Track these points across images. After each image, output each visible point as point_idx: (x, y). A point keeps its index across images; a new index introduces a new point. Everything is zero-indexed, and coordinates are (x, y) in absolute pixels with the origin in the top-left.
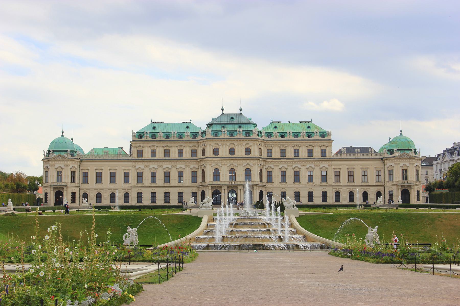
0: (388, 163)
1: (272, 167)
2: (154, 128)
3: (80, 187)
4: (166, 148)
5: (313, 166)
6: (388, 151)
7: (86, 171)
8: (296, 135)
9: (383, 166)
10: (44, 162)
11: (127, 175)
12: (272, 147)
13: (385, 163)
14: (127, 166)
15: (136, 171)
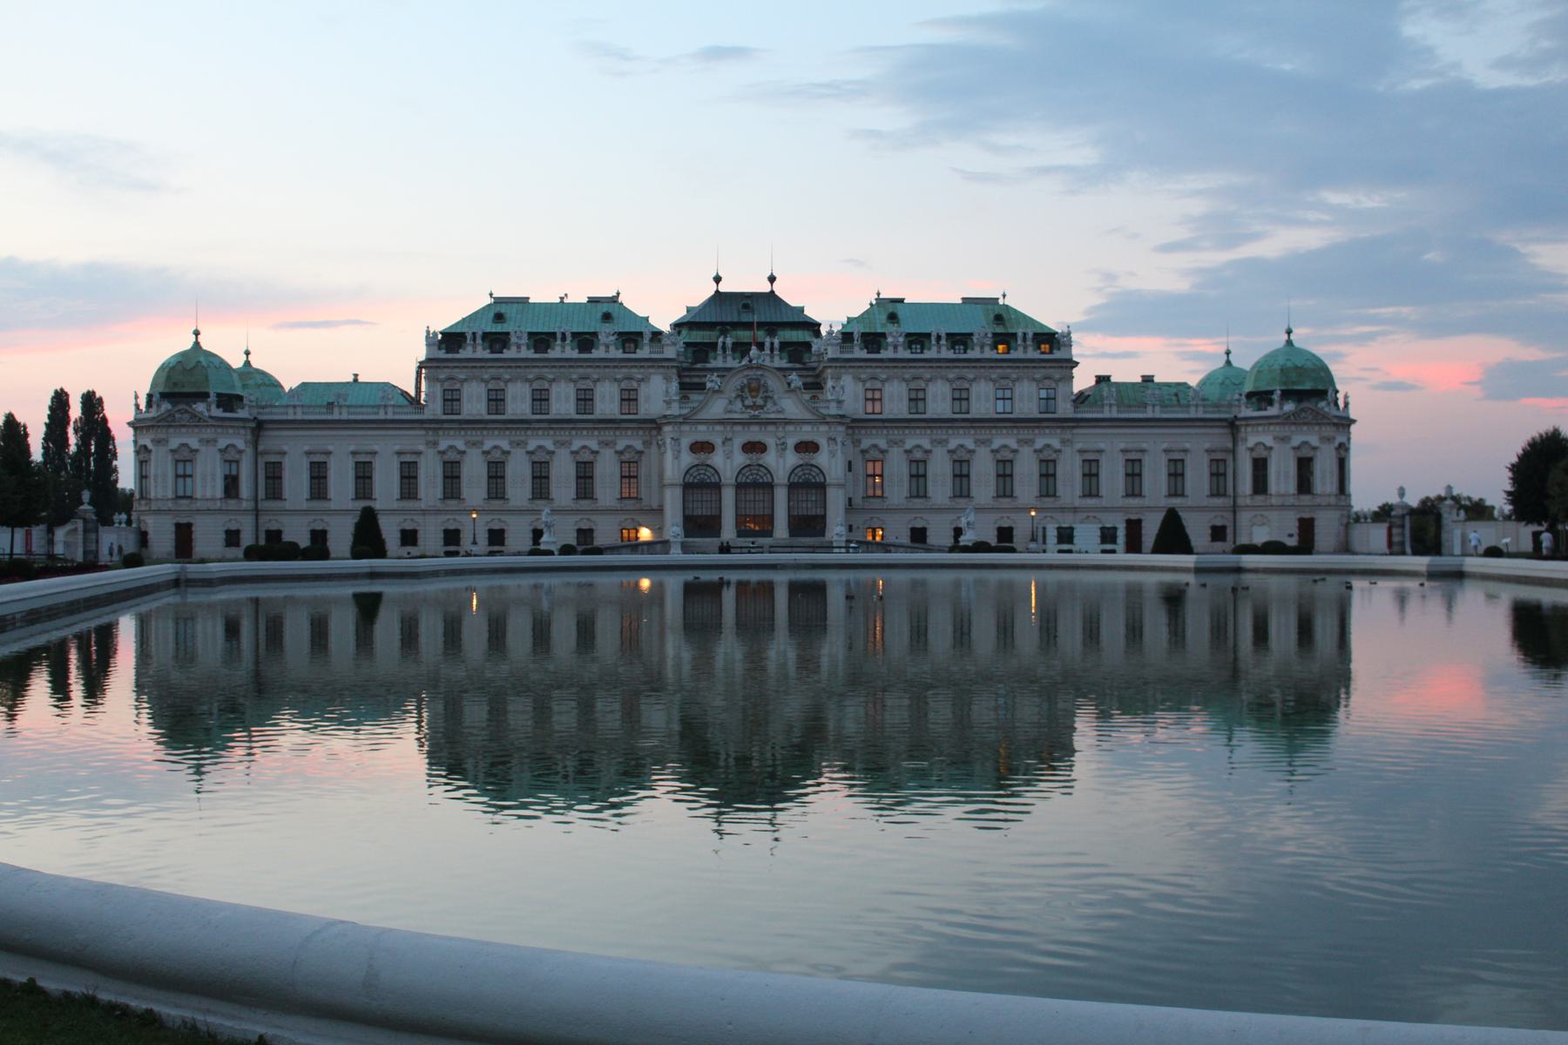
0: (1253, 438)
1: (882, 444)
2: (499, 317)
3: (257, 512)
4: (536, 385)
5: (1014, 445)
6: (1250, 395)
7: (273, 459)
8: (959, 340)
9: (1230, 445)
10: (136, 429)
11: (409, 475)
12: (883, 381)
13: (1242, 435)
14: (414, 441)
15: (438, 458)
